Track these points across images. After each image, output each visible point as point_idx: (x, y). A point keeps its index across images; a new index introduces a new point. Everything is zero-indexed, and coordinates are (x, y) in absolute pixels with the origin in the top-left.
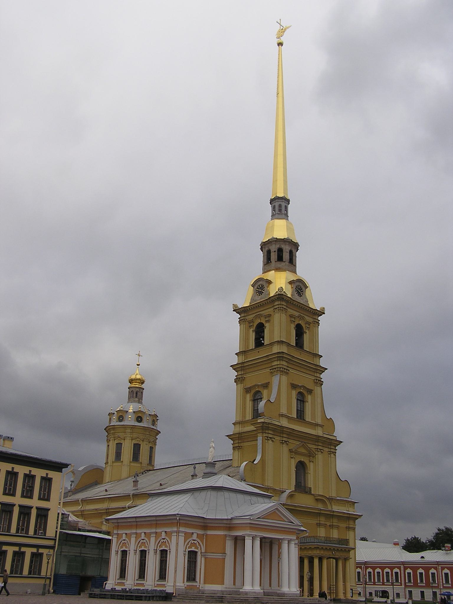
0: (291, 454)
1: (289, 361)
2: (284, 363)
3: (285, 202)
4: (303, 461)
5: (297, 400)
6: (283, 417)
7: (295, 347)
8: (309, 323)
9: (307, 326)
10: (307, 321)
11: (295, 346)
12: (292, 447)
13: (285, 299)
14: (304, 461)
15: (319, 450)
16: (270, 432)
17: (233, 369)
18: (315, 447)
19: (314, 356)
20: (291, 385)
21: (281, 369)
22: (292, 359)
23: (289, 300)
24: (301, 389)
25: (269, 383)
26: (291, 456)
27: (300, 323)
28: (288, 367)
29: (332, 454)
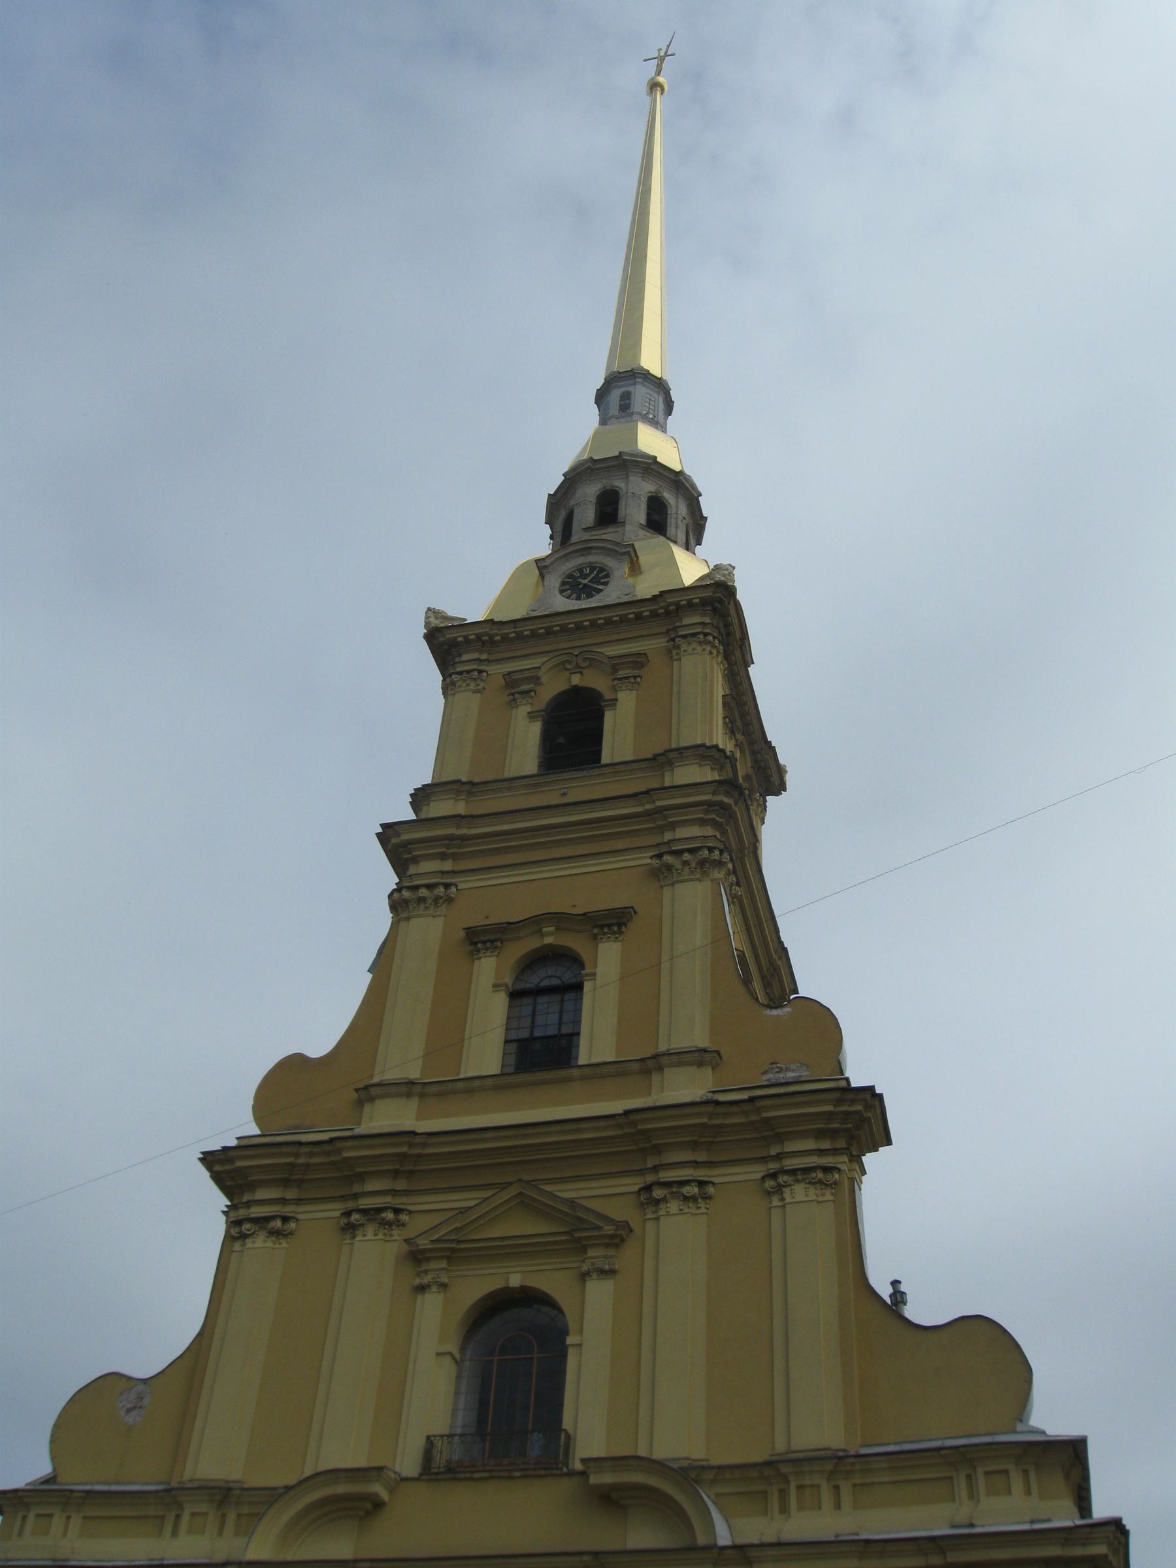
0: (424, 1267)
4: (523, 1289)
6: (377, 1102)
8: (639, 661)
12: (416, 1226)
13: (460, 639)
14: (524, 1284)
15: (658, 1193)
16: (261, 1194)
18: (633, 1184)
23: (486, 634)
24: (543, 935)
26: (417, 1281)
27: (576, 680)
28: (443, 873)
29: (799, 1189)
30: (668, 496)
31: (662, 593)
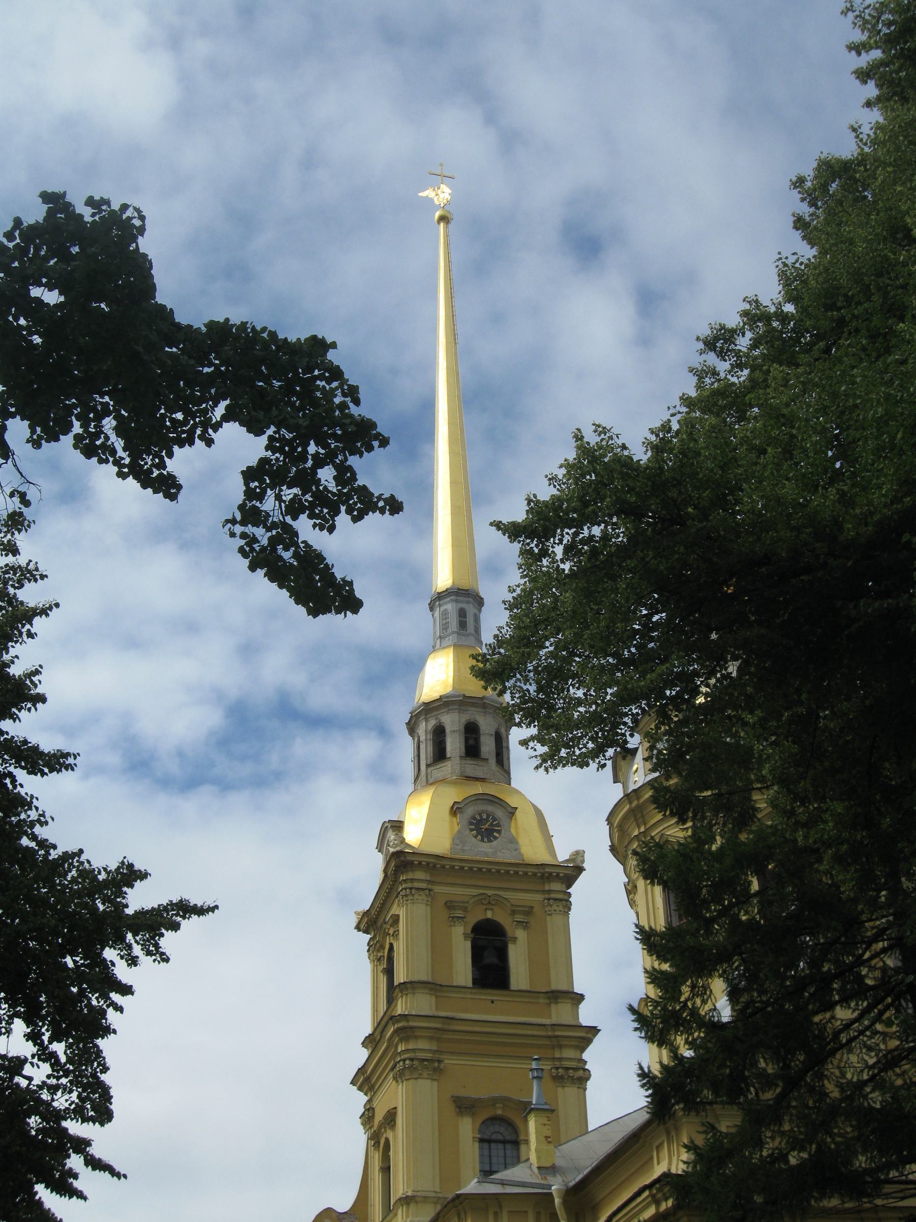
1: (437, 1035)
2: (422, 1044)
3: (457, 601)
5: (481, 1141)
7: (475, 991)
8: (529, 911)
9: (519, 918)
10: (512, 905)
11: (470, 984)
17: (360, 1089)
19: (549, 998)
20: (455, 1101)
21: (407, 1062)
22: (446, 1027)
25: (394, 1110)
27: (489, 915)
30: (503, 730)
31: (542, 864)
